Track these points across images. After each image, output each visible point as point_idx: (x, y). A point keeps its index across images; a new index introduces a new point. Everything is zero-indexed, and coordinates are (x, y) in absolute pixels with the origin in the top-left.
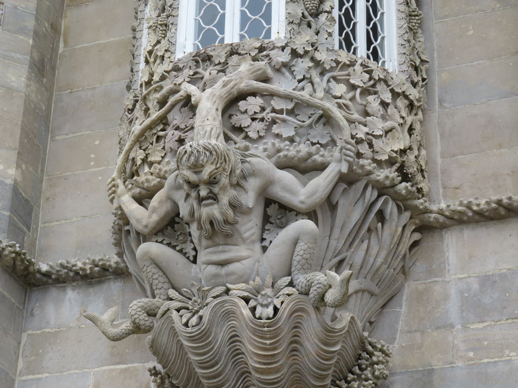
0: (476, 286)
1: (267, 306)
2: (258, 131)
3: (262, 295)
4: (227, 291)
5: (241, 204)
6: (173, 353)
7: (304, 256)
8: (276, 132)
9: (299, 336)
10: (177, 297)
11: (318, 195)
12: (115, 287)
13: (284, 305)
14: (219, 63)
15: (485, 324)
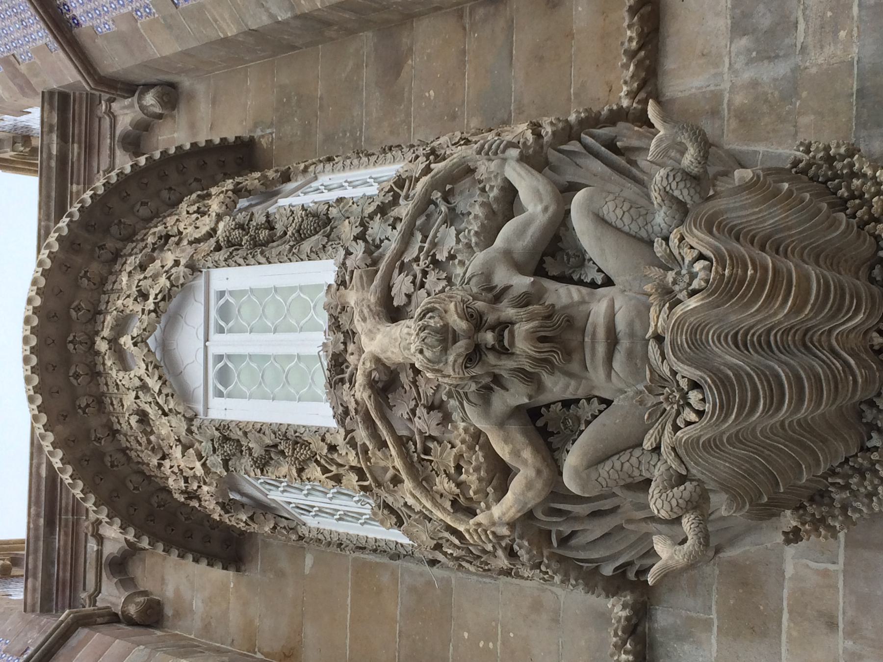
0: (744, 42)
1: (693, 276)
2: (438, 279)
3: (675, 282)
4: (659, 339)
5: (525, 293)
6: (750, 457)
7: (625, 208)
8: (446, 254)
9: (754, 237)
10: (656, 432)
11: (541, 188)
12: (663, 618)
13: (694, 244)
14: (345, 343)
15: (801, 20)
